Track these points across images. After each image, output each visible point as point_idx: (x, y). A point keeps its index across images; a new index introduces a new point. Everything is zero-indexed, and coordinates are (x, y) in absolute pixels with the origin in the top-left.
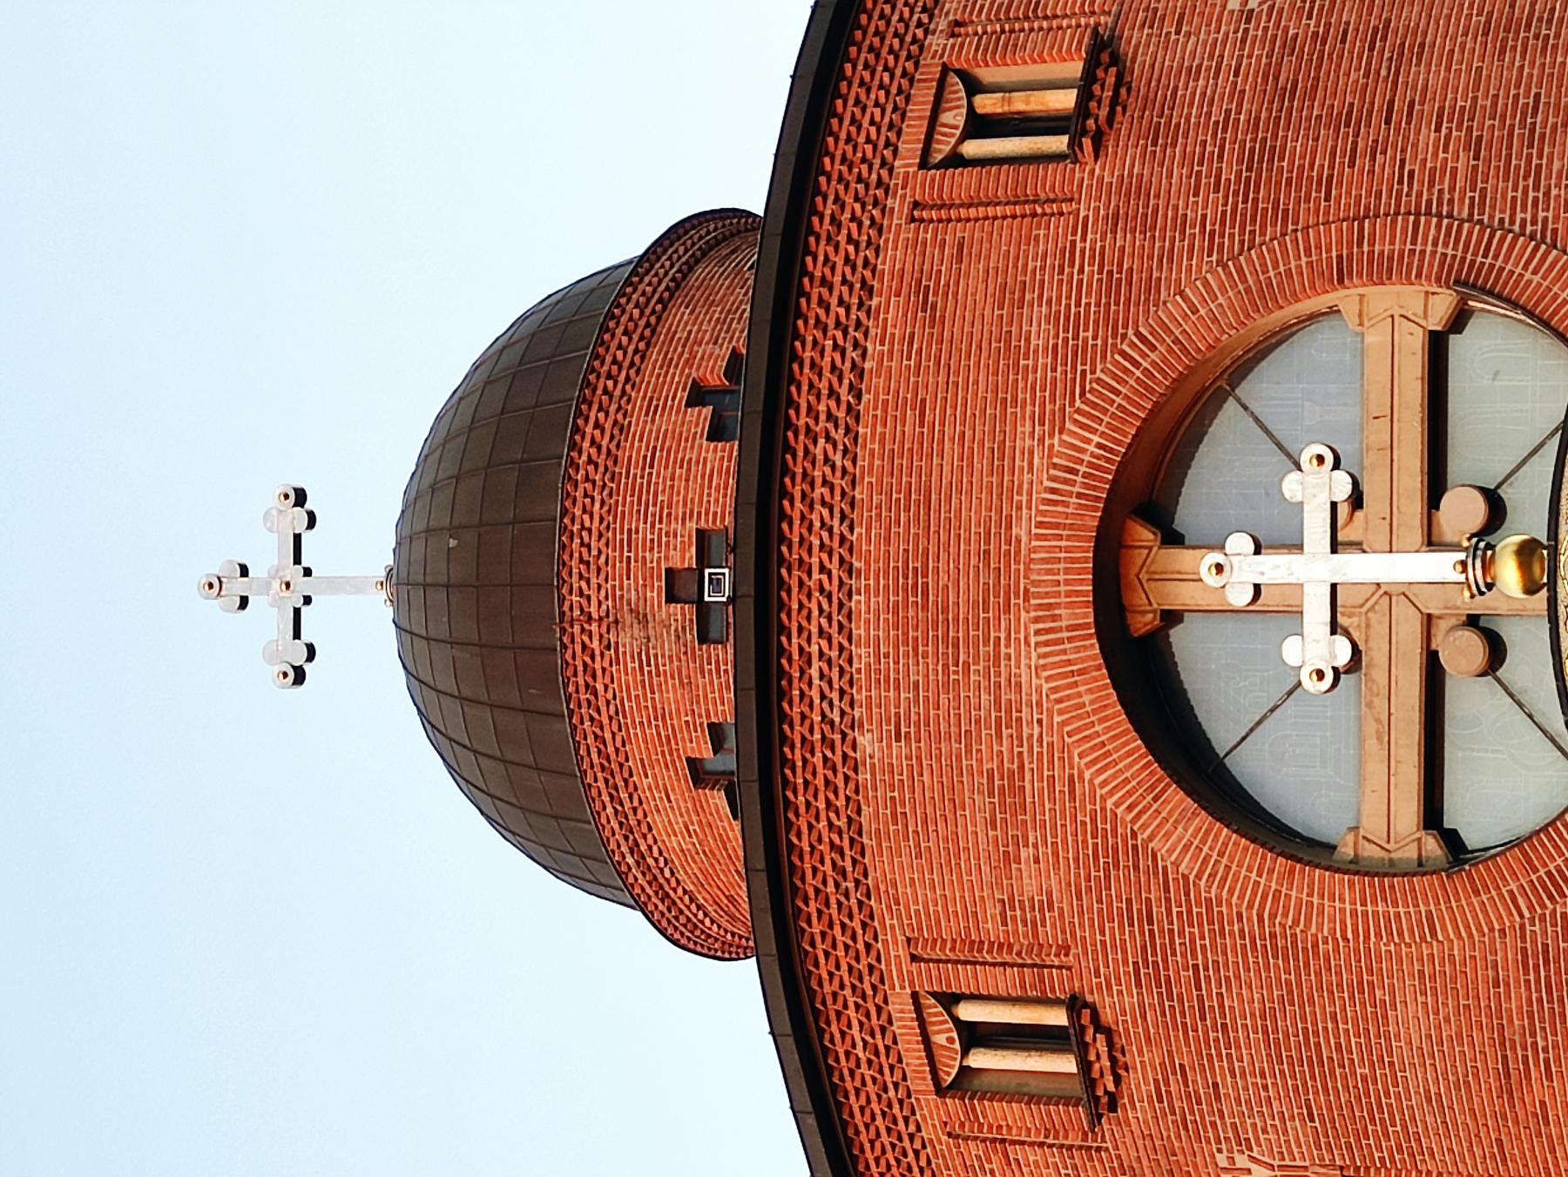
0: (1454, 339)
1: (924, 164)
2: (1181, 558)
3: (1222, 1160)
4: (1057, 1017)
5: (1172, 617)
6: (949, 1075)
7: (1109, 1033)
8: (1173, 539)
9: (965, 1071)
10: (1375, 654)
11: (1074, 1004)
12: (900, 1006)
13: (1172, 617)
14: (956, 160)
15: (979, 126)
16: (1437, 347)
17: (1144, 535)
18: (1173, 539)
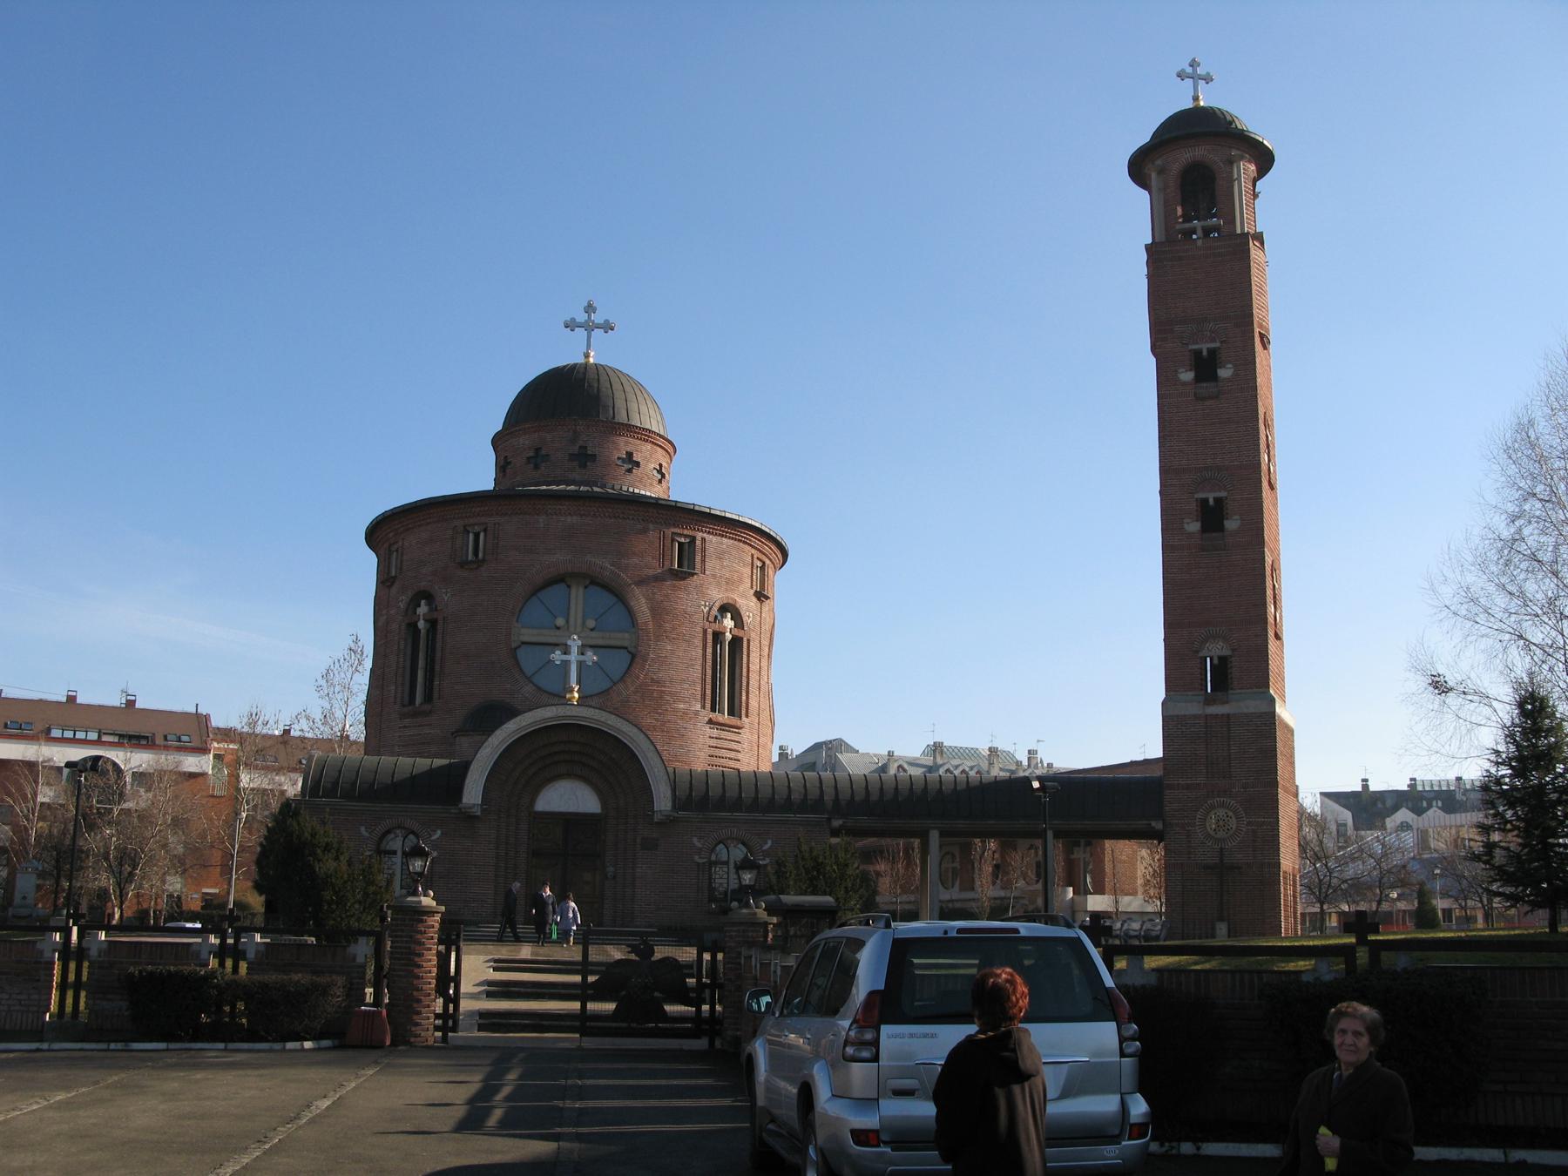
0: (626, 651)
1: (673, 533)
2: (581, 590)
3: (449, 590)
4: (481, 555)
5: (569, 586)
6: (469, 529)
7: (476, 569)
8: (586, 587)
9: (469, 532)
10: (558, 633)
11: (484, 560)
12: (483, 519)
13: (569, 586)
14: (673, 540)
15: (680, 544)
16: (626, 648)
17: (588, 582)
18: (586, 587)
